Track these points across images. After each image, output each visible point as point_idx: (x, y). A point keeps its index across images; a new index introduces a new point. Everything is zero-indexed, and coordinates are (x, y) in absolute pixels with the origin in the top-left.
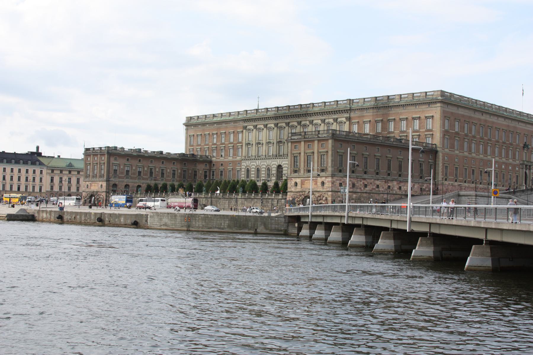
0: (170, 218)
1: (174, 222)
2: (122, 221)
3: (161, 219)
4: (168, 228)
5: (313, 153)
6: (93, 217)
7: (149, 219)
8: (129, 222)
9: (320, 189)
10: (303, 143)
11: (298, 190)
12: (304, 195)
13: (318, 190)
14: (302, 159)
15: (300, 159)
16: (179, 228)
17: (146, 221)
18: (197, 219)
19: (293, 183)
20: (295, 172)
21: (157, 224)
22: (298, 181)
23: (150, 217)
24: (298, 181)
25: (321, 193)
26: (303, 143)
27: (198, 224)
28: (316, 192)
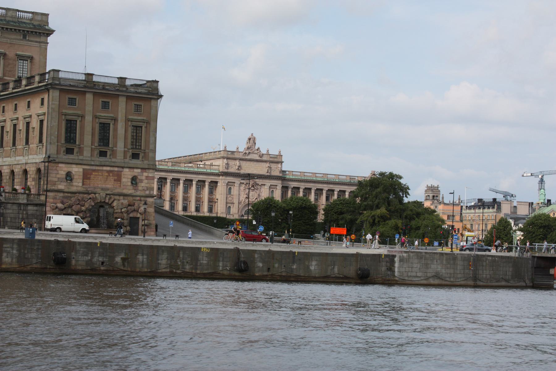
0: (444, 262)
1: (452, 271)
2: (312, 268)
3: (427, 266)
4: (444, 283)
5: (115, 120)
6: (204, 261)
7: (397, 265)
8: (351, 271)
9: (129, 190)
10: (89, 97)
11: (74, 189)
12: (93, 199)
13: (125, 192)
14: (88, 128)
15: (82, 127)
16: (463, 283)
17: (391, 268)
18: (484, 264)
20: (69, 151)
21: (419, 274)
22: (77, 170)
23: (401, 260)
24: (77, 170)
25: (131, 199)
26: (89, 97)
27: (485, 273)
28: (120, 195)
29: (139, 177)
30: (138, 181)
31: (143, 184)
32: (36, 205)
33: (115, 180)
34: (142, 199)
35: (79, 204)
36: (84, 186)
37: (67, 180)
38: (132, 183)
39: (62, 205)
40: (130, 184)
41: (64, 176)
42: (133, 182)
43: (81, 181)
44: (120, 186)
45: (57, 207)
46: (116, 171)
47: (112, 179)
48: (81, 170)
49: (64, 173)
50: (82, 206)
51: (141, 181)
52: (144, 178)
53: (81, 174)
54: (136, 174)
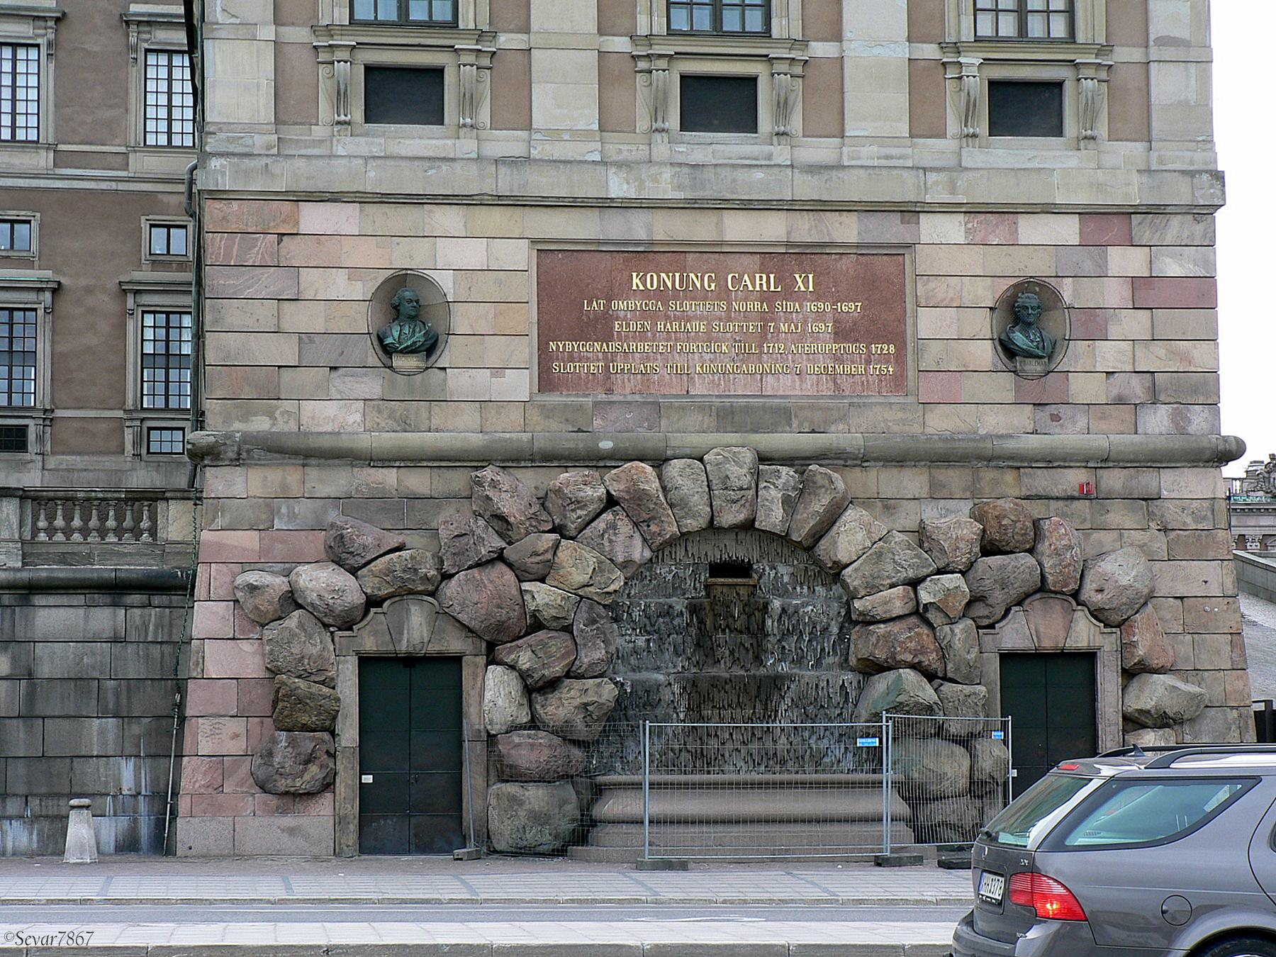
19: (341, 294)
29: (1067, 291)
30: (1053, 325)
31: (1110, 354)
32: (114, 590)
33: (843, 333)
34: (1114, 480)
35: (500, 557)
36: (554, 399)
37: (388, 351)
38: (1008, 350)
39: (342, 579)
40: (985, 353)
41: (360, 319)
42: (1019, 338)
43: (526, 350)
44: (898, 382)
45: (292, 600)
46: (843, 250)
47: (811, 316)
48: (519, 255)
49: (362, 290)
50: (522, 575)
51: (1094, 325)
52: (1114, 294)
53: (527, 288)
54: (1038, 266)
